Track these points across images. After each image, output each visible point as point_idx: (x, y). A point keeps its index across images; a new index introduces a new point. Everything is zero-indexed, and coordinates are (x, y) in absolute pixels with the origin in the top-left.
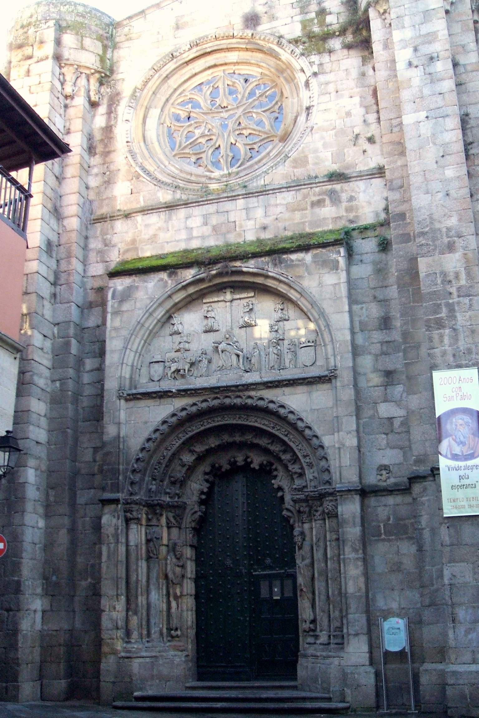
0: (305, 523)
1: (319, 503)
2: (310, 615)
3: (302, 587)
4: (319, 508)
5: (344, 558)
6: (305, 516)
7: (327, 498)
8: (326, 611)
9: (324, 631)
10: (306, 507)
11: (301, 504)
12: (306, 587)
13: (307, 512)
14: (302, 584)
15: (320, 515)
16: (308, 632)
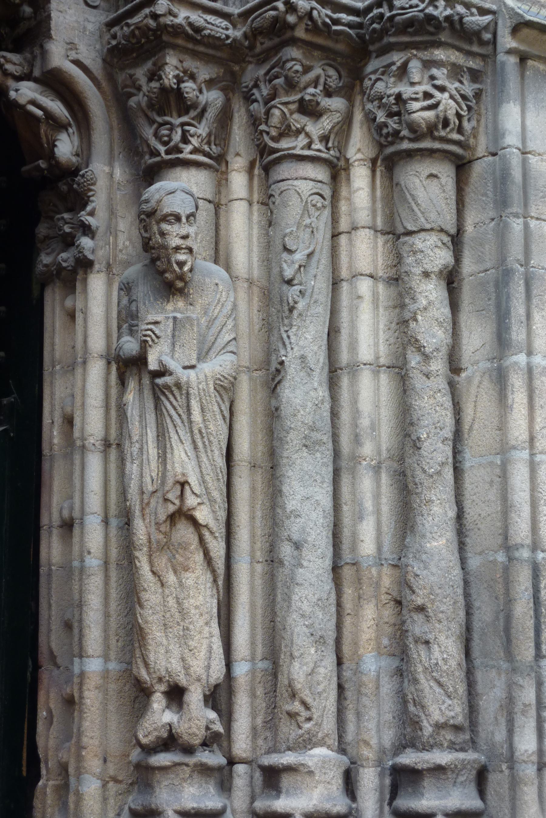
0: (187, 164)
1: (332, 72)
2: (210, 650)
3: (191, 501)
4: (325, 102)
5: (530, 370)
6: (202, 129)
7: (440, 54)
8: (331, 635)
9: (322, 743)
10: (210, 83)
11: (191, 64)
12: (212, 501)
13: (211, 114)
14: (193, 480)
15: (325, 139)
16: (189, 750)
